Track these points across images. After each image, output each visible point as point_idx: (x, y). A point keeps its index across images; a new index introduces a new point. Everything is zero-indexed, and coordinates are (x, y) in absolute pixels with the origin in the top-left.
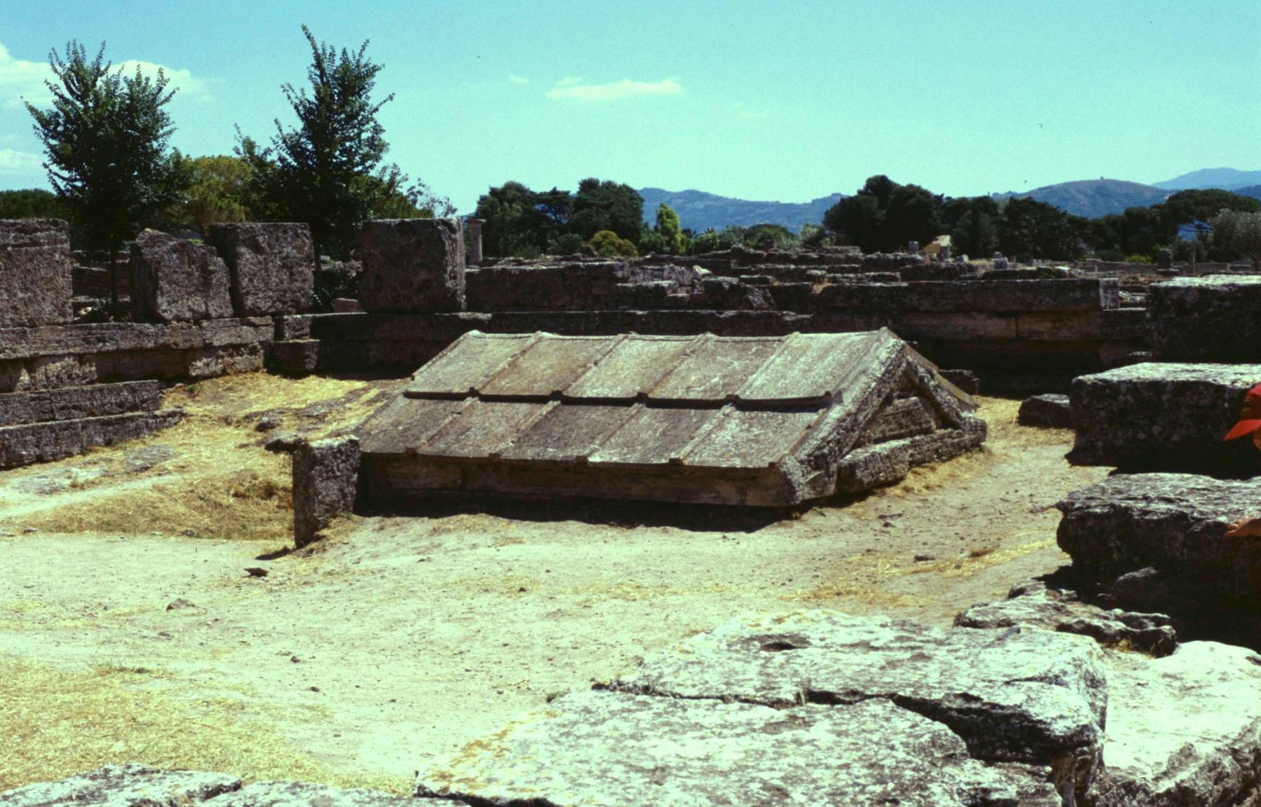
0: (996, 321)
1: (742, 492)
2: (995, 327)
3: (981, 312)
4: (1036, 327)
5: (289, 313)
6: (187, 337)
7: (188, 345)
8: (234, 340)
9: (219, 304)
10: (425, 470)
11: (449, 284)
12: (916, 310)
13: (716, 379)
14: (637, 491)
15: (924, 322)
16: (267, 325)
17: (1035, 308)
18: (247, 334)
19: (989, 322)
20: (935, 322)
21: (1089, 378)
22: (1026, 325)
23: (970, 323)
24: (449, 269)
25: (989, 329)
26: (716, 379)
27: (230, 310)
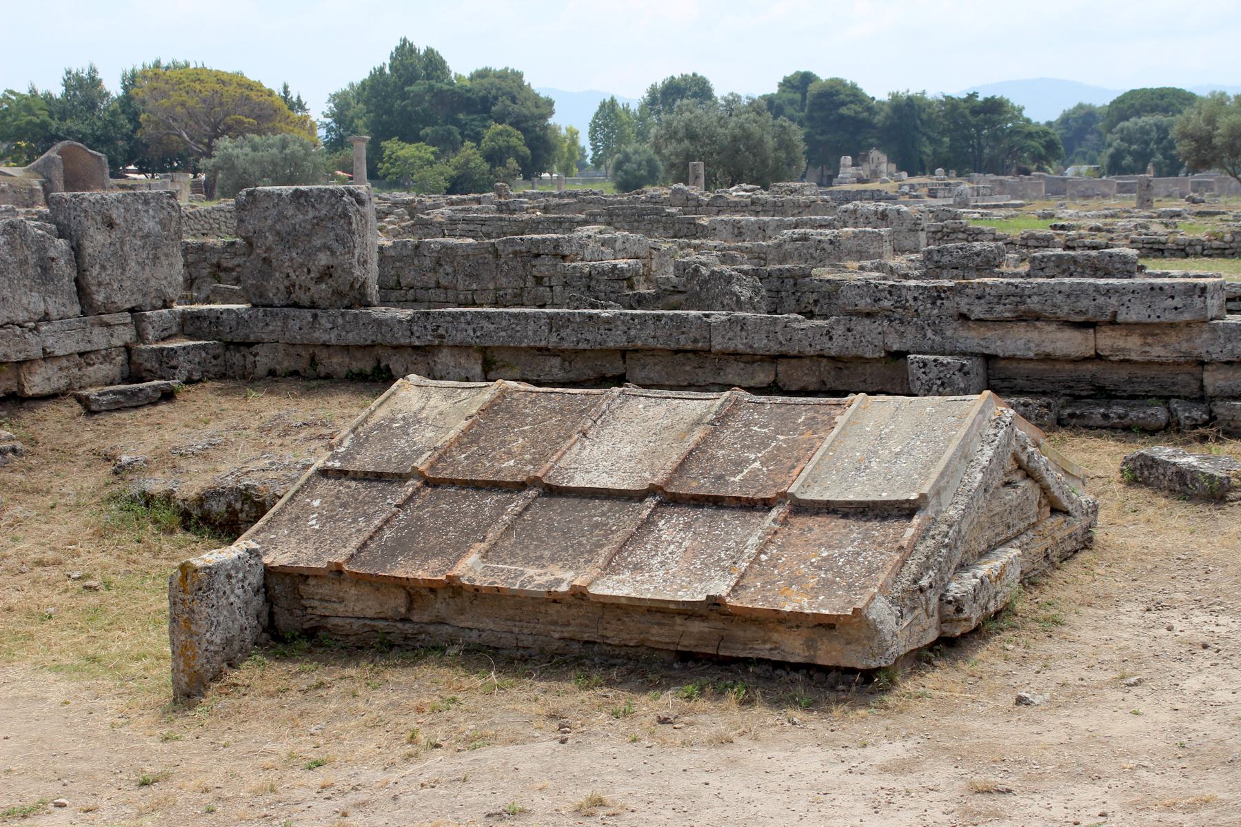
1: (810, 644)
3: (1048, 320)
4: (1121, 343)
5: (154, 308)
6: (21, 346)
7: (22, 357)
8: (84, 347)
9: (63, 304)
10: (353, 591)
11: (357, 272)
12: (964, 317)
13: (757, 465)
14: (658, 634)
15: (973, 333)
16: (125, 325)
17: (1120, 319)
18: (99, 339)
19: (1059, 335)
20: (989, 334)
22: (1107, 341)
23: (1034, 335)
24: (357, 252)
25: (1059, 344)
26: (757, 465)
27: (77, 309)
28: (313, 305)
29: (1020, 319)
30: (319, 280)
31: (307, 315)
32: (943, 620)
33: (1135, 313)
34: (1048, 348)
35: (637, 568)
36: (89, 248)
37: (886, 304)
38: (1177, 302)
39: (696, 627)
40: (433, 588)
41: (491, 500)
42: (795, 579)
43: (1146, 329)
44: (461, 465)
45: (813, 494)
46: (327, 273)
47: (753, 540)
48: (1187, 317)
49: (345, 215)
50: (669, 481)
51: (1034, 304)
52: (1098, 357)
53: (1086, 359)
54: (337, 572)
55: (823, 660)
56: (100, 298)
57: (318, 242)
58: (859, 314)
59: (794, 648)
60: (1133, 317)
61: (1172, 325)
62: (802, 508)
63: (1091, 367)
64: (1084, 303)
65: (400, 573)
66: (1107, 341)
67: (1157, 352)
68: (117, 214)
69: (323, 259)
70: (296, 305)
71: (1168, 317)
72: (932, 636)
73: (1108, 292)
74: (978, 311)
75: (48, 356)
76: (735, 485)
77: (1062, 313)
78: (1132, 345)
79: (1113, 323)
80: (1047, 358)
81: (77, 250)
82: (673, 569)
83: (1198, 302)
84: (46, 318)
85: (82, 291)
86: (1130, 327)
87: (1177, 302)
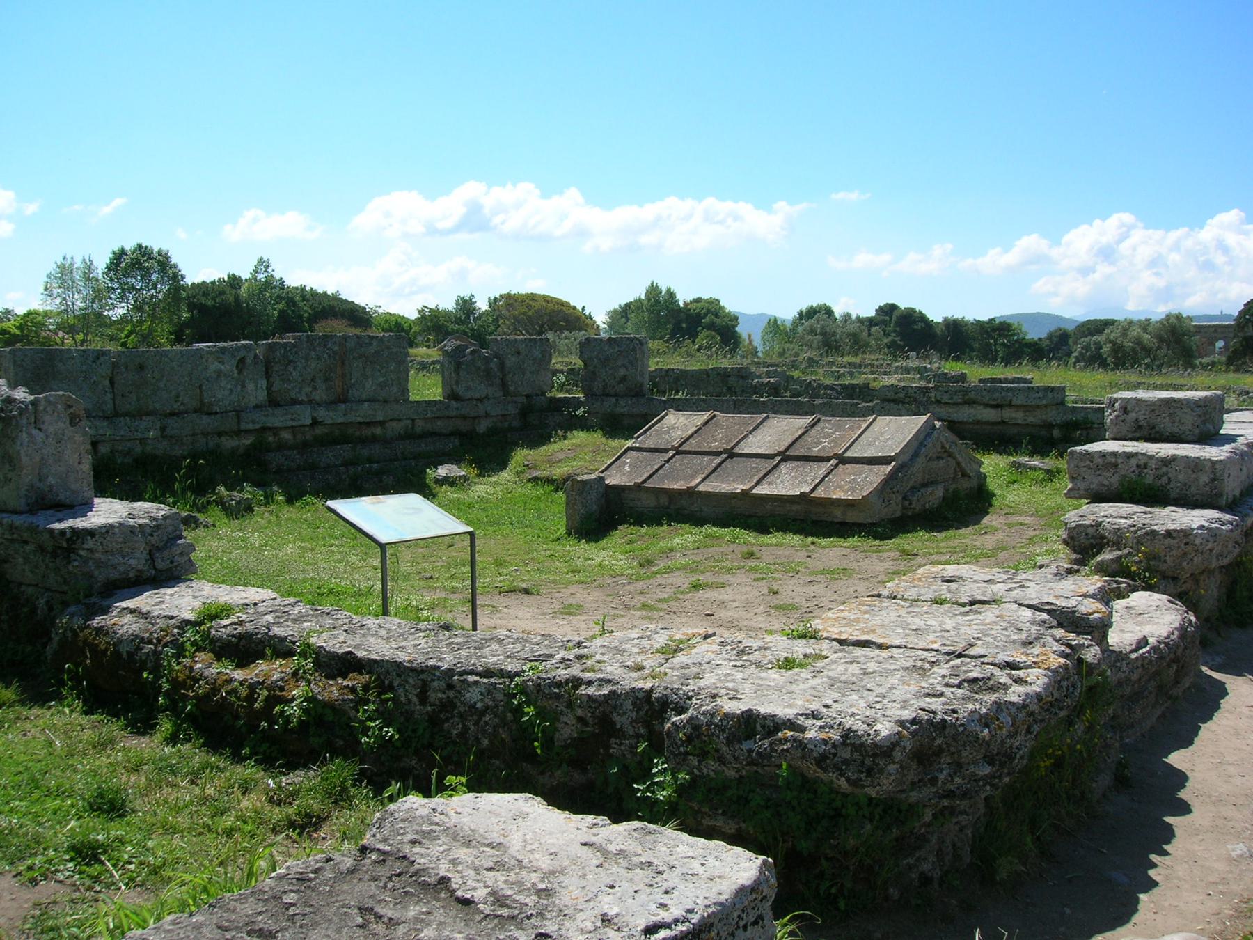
0: (989, 410)
2: (989, 415)
3: (980, 404)
11: (639, 379)
12: (938, 402)
21: (1078, 449)
22: (1008, 414)
23: (972, 411)
28: (616, 395)
29: (965, 403)
30: (619, 383)
31: (614, 400)
32: (904, 508)
33: (1019, 400)
34: (979, 418)
35: (770, 483)
36: (508, 364)
37: (901, 395)
38: (1040, 395)
39: (795, 507)
40: (680, 492)
41: (706, 458)
42: (841, 487)
43: (1026, 408)
44: (693, 445)
45: (848, 454)
46: (624, 379)
47: (821, 473)
48: (1044, 402)
49: (634, 349)
50: (786, 450)
51: (972, 395)
52: (1003, 422)
53: (998, 423)
54: (638, 486)
55: (849, 520)
56: (512, 388)
57: (619, 363)
58: (889, 401)
59: (838, 514)
60: (1019, 402)
61: (1038, 407)
62: (842, 460)
63: (1000, 427)
64: (997, 395)
65: (666, 486)
66: (1008, 414)
67: (1031, 420)
68: (522, 347)
69: (622, 372)
70: (608, 395)
71: (1038, 402)
72: (898, 514)
73: (1008, 389)
74: (945, 399)
75: (487, 415)
76: (816, 451)
77: (986, 400)
78: (1018, 416)
79: (1010, 405)
80: (978, 422)
81: (502, 365)
82: (787, 483)
83: (1050, 395)
84: (487, 397)
85: (504, 385)
86: (1018, 407)
87: (1040, 395)
